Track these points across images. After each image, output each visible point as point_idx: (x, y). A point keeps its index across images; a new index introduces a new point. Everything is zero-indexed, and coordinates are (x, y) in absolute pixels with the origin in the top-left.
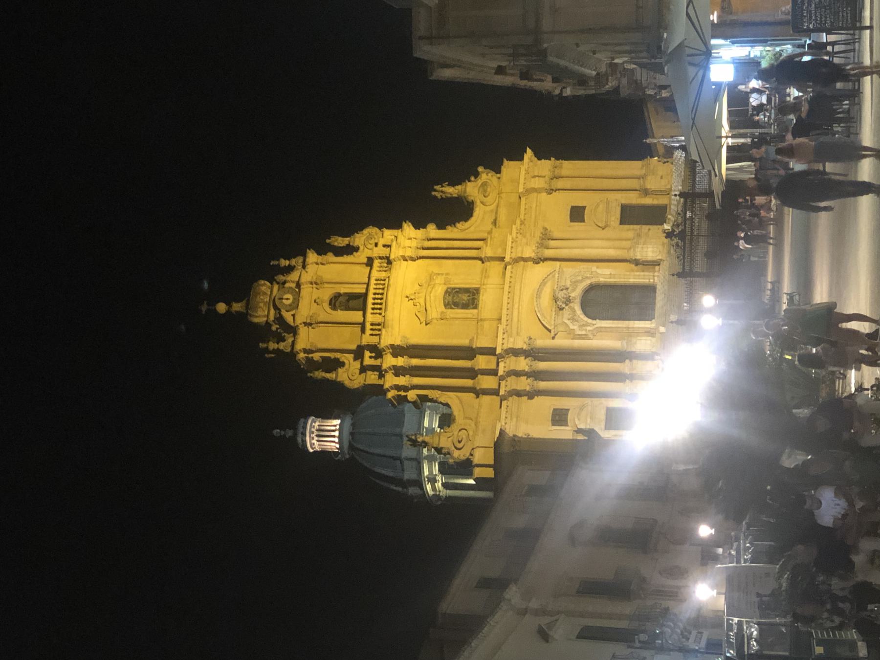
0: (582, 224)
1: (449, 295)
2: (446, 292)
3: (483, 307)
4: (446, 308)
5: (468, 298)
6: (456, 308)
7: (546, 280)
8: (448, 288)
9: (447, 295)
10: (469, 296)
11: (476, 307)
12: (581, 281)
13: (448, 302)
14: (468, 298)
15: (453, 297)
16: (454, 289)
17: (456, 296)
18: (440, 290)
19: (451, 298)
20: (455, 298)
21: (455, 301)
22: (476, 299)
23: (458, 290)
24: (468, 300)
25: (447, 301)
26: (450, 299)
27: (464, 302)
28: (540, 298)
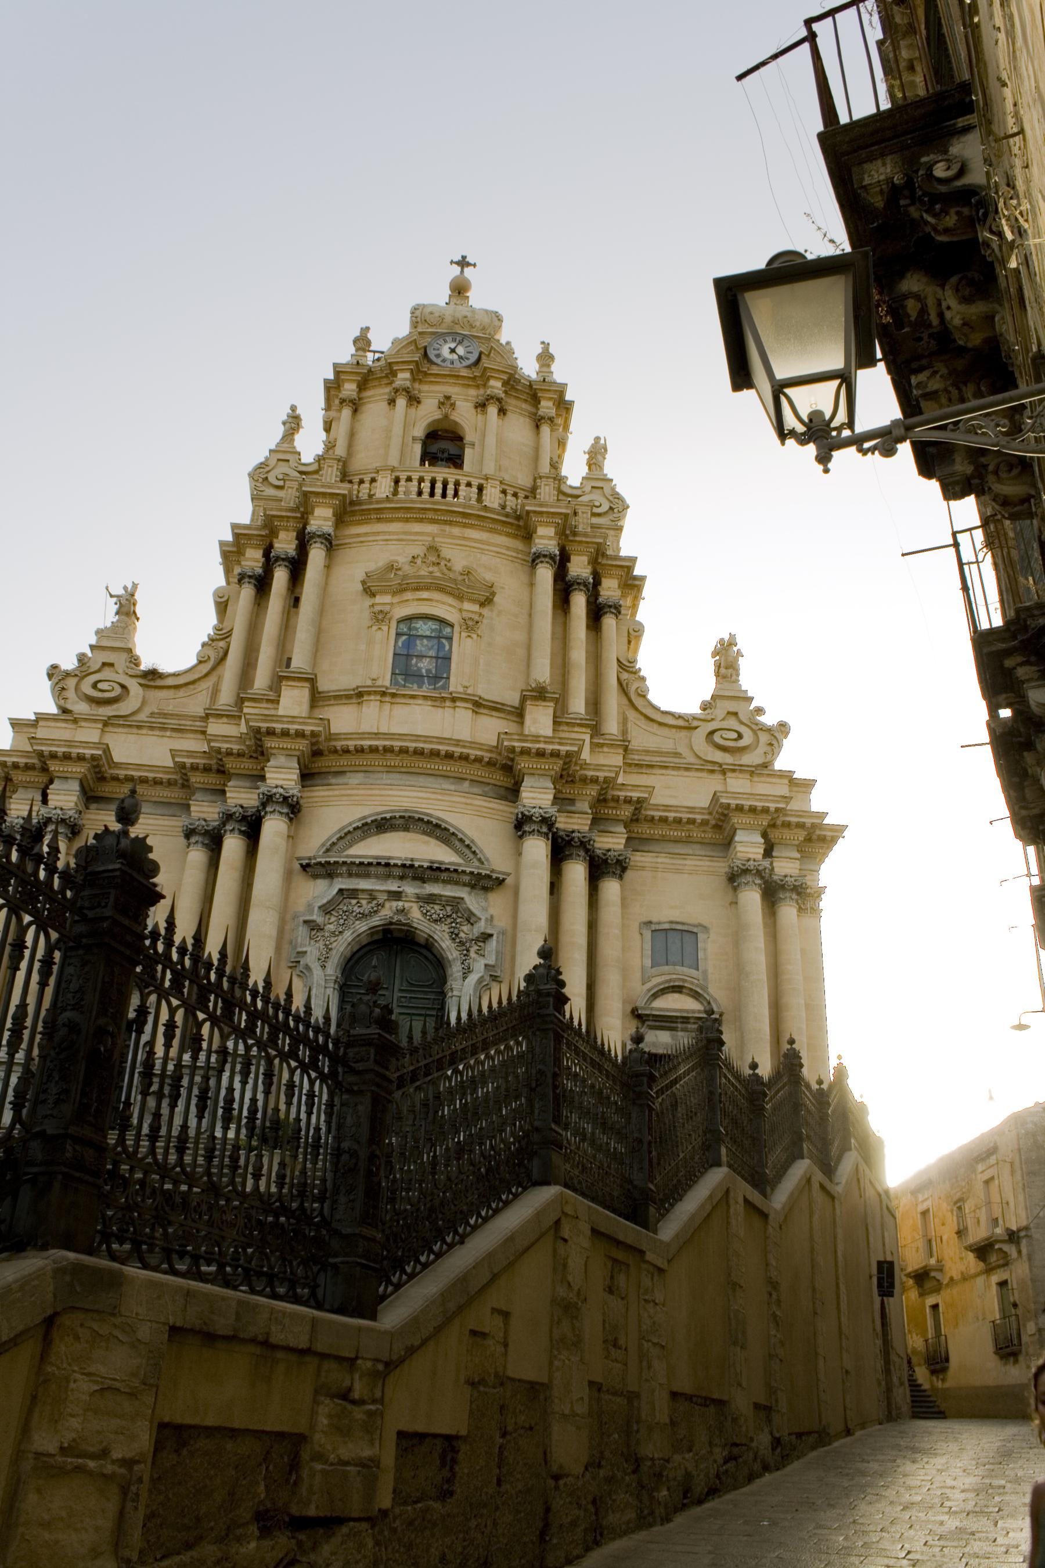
0: (648, 962)
1: (433, 630)
2: (442, 621)
3: (398, 700)
4: (399, 622)
5: (424, 671)
6: (400, 644)
7: (457, 843)
8: (452, 626)
9: (434, 627)
10: (428, 671)
11: (394, 682)
12: (454, 936)
13: (416, 629)
14: (424, 671)
15: (426, 637)
16: (450, 639)
17: (430, 645)
18: (445, 608)
19: (428, 633)
20: (425, 641)
21: (418, 642)
22: (420, 686)
23: (447, 648)
24: (419, 669)
25: (418, 626)
26: (424, 628)
27: (414, 661)
28: (406, 829)
